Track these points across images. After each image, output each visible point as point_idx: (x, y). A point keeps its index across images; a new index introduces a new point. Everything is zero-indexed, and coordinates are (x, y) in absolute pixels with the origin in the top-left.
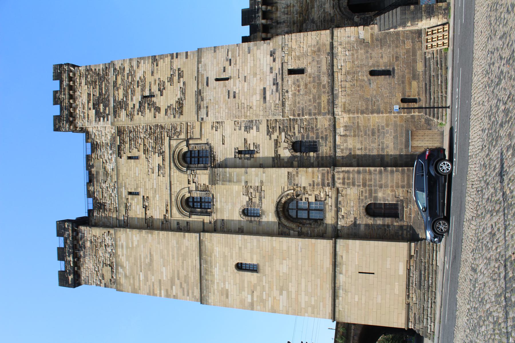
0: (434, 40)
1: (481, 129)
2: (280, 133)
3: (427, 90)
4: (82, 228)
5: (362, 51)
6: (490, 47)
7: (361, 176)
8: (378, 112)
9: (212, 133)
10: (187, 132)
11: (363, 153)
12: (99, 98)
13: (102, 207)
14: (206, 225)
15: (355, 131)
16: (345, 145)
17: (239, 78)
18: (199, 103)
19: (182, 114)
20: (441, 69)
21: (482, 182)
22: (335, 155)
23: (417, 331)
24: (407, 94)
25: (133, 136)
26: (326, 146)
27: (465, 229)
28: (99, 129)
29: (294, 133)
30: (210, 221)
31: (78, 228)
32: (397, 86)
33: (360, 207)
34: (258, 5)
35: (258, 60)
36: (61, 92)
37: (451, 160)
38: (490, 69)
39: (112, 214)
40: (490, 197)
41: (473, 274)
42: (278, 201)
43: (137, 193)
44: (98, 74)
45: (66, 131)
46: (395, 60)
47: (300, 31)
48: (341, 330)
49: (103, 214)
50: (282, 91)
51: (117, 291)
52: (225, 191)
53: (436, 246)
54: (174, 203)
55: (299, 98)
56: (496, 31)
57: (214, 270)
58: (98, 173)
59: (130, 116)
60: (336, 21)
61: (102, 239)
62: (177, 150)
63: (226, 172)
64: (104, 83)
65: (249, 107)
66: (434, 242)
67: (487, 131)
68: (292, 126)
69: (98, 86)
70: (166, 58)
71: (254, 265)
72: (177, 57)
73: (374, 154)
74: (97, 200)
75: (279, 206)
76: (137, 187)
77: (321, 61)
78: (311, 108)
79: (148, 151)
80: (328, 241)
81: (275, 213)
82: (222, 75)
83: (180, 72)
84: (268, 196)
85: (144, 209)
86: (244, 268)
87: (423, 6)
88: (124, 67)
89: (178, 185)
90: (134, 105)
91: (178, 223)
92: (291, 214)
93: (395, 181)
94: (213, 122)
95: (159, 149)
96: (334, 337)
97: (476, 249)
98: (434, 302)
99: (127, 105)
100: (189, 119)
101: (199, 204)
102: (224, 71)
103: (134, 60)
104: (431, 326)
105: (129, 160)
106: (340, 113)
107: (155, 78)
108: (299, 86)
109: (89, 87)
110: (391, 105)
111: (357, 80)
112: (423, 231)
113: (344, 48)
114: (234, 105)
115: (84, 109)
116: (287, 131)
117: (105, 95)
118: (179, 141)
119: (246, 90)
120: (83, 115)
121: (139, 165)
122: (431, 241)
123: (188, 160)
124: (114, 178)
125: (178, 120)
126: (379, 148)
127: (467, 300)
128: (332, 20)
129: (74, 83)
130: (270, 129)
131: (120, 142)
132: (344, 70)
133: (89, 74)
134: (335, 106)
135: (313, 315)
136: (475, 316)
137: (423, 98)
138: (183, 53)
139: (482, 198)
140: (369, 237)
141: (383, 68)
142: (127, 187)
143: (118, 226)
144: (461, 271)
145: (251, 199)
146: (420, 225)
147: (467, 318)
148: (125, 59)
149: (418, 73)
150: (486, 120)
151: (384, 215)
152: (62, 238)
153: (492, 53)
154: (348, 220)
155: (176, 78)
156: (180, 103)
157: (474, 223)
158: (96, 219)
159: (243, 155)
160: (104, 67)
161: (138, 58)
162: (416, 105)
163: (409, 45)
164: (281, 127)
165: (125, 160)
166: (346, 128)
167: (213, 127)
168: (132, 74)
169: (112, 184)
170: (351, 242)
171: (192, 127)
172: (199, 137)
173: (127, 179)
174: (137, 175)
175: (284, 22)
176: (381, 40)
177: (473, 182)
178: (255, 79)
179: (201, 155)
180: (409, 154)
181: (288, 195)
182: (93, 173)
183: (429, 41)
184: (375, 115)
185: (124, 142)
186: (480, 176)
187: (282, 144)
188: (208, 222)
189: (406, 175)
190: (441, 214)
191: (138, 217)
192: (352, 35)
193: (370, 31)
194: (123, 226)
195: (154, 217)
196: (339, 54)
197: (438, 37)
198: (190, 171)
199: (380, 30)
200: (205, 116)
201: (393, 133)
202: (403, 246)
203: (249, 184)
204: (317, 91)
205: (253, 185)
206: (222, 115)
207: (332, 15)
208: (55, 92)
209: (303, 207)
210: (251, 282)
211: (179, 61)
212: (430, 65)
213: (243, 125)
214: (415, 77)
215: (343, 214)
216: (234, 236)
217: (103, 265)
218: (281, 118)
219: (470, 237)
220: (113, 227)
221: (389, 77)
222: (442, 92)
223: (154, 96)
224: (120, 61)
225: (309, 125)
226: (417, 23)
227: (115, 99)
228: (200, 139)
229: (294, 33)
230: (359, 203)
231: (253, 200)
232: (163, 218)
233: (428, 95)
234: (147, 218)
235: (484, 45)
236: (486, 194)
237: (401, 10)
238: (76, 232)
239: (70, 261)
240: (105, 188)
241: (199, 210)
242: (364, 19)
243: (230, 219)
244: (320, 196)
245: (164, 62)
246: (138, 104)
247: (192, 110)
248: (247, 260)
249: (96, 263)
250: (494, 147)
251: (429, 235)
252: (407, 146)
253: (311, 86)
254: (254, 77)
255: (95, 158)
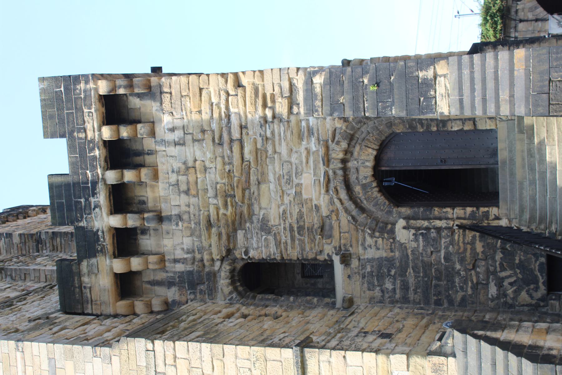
34: (94, 168)
175: (179, 217)
207: (325, 212)
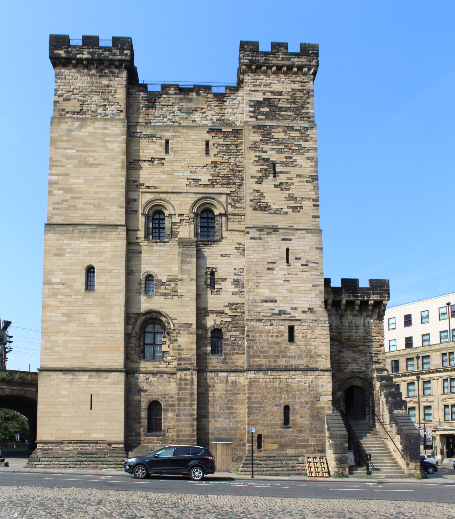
0: (315, 464)
1: (232, 505)
2: (230, 317)
3: (269, 458)
4: (124, 75)
5: (308, 399)
6: (307, 512)
7: (188, 397)
8: (249, 413)
9: (233, 243)
10: (234, 215)
11: (210, 399)
12: (276, 106)
13: (151, 104)
14: (134, 233)
15: (231, 390)
16: (218, 381)
17: (288, 274)
18: (265, 230)
19: (253, 210)
20: (288, 470)
21: (184, 507)
22: (208, 372)
23: (34, 451)
24: (265, 440)
25: (232, 150)
26: (217, 362)
27: (139, 493)
28: (241, 105)
29: (230, 331)
30: (139, 238)
31: (125, 68)
32: (273, 430)
33: (158, 395)
35: (305, 295)
36: (286, 54)
37: (203, 479)
38: (287, 512)
39: (143, 117)
40: (169, 514)
41: (96, 501)
42: (162, 313)
43: (167, 151)
44: (303, 107)
45: (240, 59)
46: (298, 429)
47: (331, 339)
48: (29, 377)
49: (142, 105)
50: (272, 319)
51: (51, 117)
52: (172, 256)
53: (122, 468)
54: (158, 196)
55: (265, 336)
56: (320, 517)
57: (85, 240)
58: (190, 100)
59: (254, 147)
60: (339, 374)
61: (112, 102)
62: (215, 202)
63: (191, 258)
64: (292, 113)
65: (257, 284)
66: (125, 466)
67: (230, 510)
68: (237, 329)
69: (289, 106)
70: (314, 193)
71: (93, 286)
72: (314, 205)
73: (209, 408)
74: (159, 98)
75: (157, 314)
76: (174, 152)
77: (301, 359)
78: (255, 348)
79: (215, 167)
80: (123, 364)
81: (150, 310)
82: (292, 256)
83: (299, 208)
84: (168, 303)
85: (150, 159)
86: (89, 275)
87: (347, 455)
88: (308, 141)
89: (177, 202)
90: (266, 152)
91: (135, 200)
92: (149, 326)
93: (183, 428)
94: (244, 245)
95: (217, 181)
96: (21, 370)
97: (120, 503)
98: (66, 467)
99: (267, 144)
100: (248, 218)
101: (157, 226)
102: (296, 259)
103: (315, 154)
104: (41, 464)
105: (205, 143)
106: (249, 377)
107: (294, 179)
108: (277, 336)
109: (290, 94)
110: (256, 425)
111: (280, 393)
112: (135, 455)
113: (312, 382)
114: (261, 268)
115: (264, 85)
116: (233, 324)
117: (279, 114)
118: (225, 205)
119: (275, 281)
120: (257, 84)
121: (199, 155)
122: (126, 463)
123: (205, 215)
124: (185, 121)
125: (248, 204)
126: (215, 413)
127: (69, 497)
128: (339, 370)
129: (296, 73)
130: (234, 306)
131: (225, 132)
132: (290, 381)
133: (304, 94)
134: (256, 372)
135: (43, 348)
136: (55, 504)
137: (262, 454)
138: (318, 213)
139: (169, 507)
140: (128, 404)
141: (291, 418)
142: (175, 139)
143: (130, 124)
144: (98, 491)
145: (164, 285)
146: (142, 452)
147: (52, 498)
148: (317, 143)
149: (286, 449)
150: (240, 510)
151: (150, 419)
152: (110, 45)
153: (301, 514)
154: (144, 384)
155: (292, 203)
156: (265, 208)
157: (145, 501)
158: (136, 94)
159: (209, 276)
160: (310, 115)
161: (317, 158)
162: (255, 448)
163: (312, 441)
164: (237, 318)
165: (205, 137)
166: (235, 383)
167: (240, 245)
168: (301, 150)
169: (177, 119)
170: (122, 386)
171: (240, 220)
172: (229, 229)
173: (183, 139)
174: (188, 152)
176: (318, 416)
177: (184, 499)
178: (286, 291)
179: (210, 230)
180: (210, 442)
181: (169, 323)
182: (190, 94)
183: (314, 459)
184: (247, 410)
185: (227, 137)
186: (189, 505)
187: (220, 318)
188: (138, 236)
189: (189, 438)
190: (152, 471)
191: (141, 151)
192: (324, 390)
193: (327, 406)
194: (130, 131)
195: (141, 171)
196: (306, 377)
197: (318, 467)
198: (193, 217)
199: (327, 416)
200: (250, 235)
201: (229, 427)
202: (120, 437)
203: (179, 283)
204: (271, 355)
205: (178, 286)
206: (251, 254)
208: (285, 46)
209: (156, 339)
210: (74, 282)
211: (311, 208)
212: (292, 460)
213: (240, 278)
214: (282, 447)
215: (150, 379)
216: (124, 265)
217: (81, 101)
218: (246, 318)
219: (131, 498)
220: (128, 117)
221: (282, 424)
222: (267, 471)
223: (274, 177)
224: (315, 136)
225: (238, 346)
226: (332, 449)
227: (273, 128)
228: (227, 230)
229: (330, 332)
230: (161, 395)
231: (163, 287)
232: (141, 182)
233: (264, 458)
234: (140, 162)
235: (308, 507)
236: (173, 511)
237: (344, 435)
238: (120, 65)
239: (83, 54)
240: (173, 109)
241: (151, 226)
242: (339, 400)
243: (142, 261)
244: (168, 357)
245: (311, 190)
246: (266, 157)
247: (258, 221)
248: (98, 279)
249: (82, 91)
250: (216, 517)
251: (132, 460)
252: (217, 439)
253: (277, 348)
254: (288, 290)
255: (207, 98)
